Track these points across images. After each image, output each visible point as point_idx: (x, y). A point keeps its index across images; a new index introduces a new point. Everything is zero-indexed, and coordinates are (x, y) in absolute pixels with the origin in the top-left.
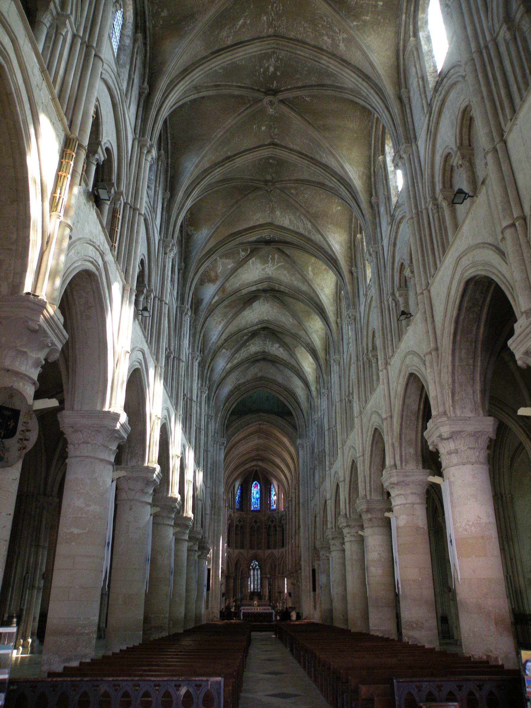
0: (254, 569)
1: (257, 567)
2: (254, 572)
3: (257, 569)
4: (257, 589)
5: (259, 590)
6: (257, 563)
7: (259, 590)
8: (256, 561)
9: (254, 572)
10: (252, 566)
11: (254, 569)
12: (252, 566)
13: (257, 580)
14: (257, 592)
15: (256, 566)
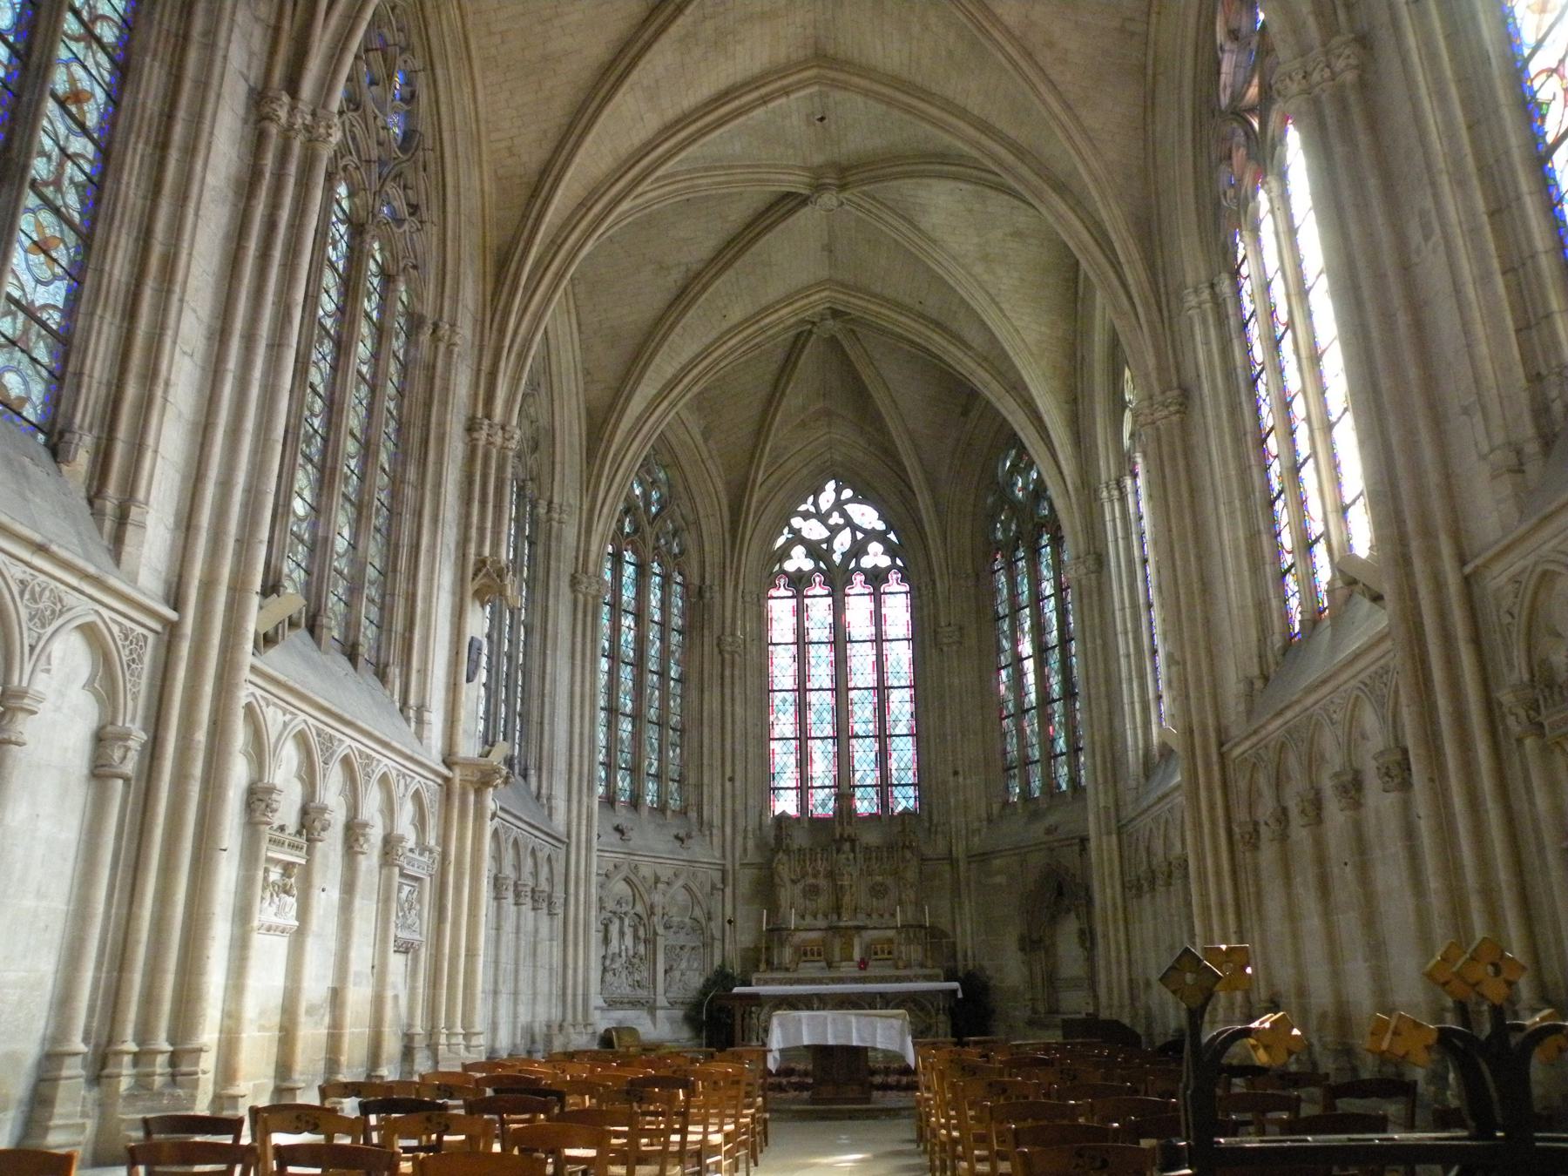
0: (837, 581)
1: (876, 556)
2: (838, 609)
3: (876, 578)
4: (884, 787)
5: (905, 800)
6: (867, 516)
7: (905, 800)
8: (862, 497)
9: (838, 609)
10: (816, 551)
11: (837, 581)
12: (814, 550)
13: (881, 690)
14: (884, 817)
15: (858, 550)
